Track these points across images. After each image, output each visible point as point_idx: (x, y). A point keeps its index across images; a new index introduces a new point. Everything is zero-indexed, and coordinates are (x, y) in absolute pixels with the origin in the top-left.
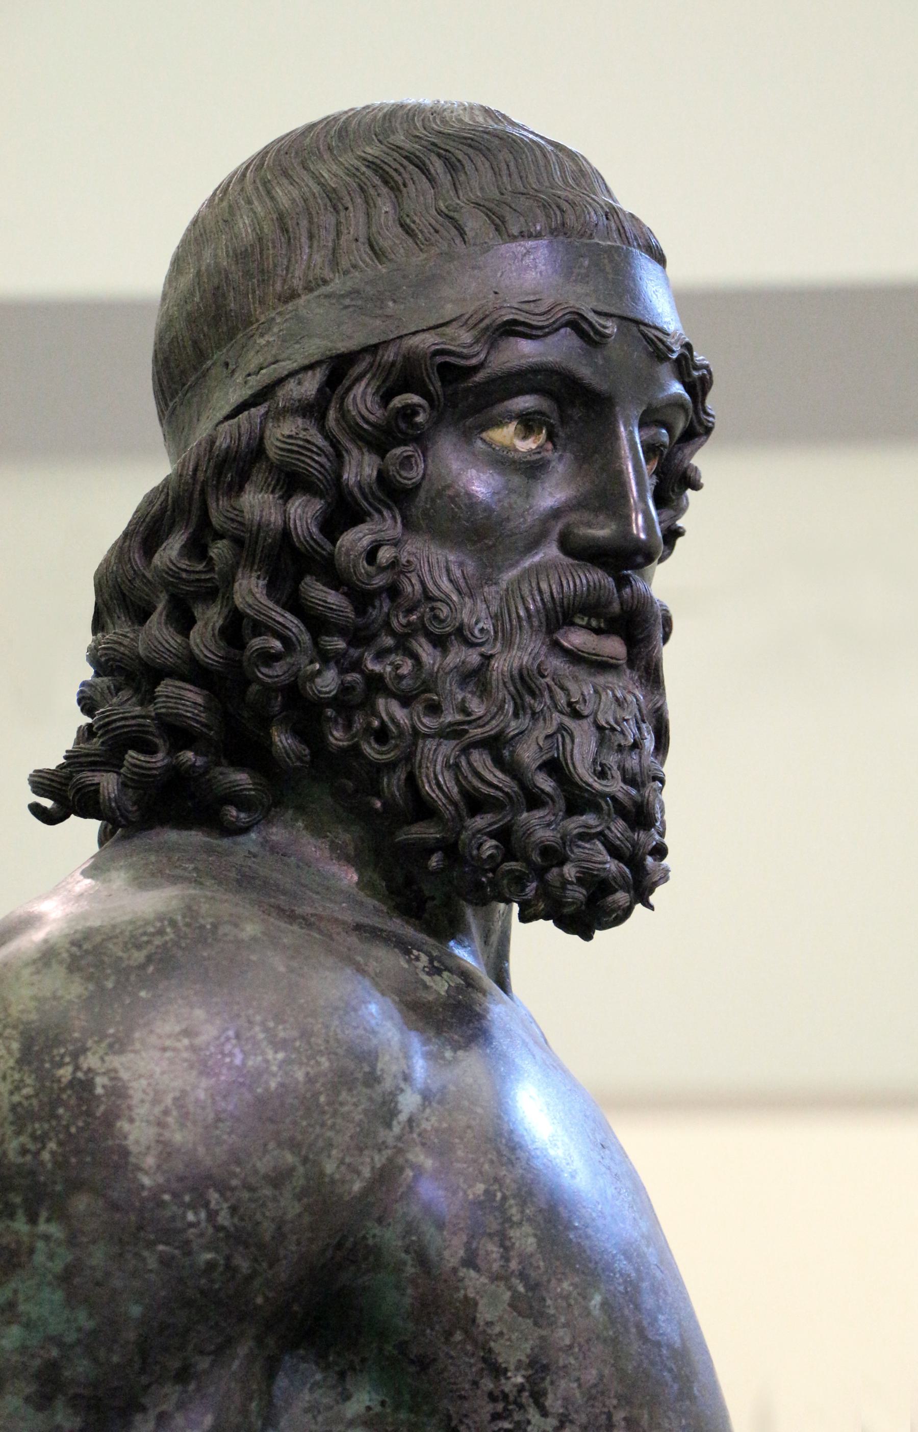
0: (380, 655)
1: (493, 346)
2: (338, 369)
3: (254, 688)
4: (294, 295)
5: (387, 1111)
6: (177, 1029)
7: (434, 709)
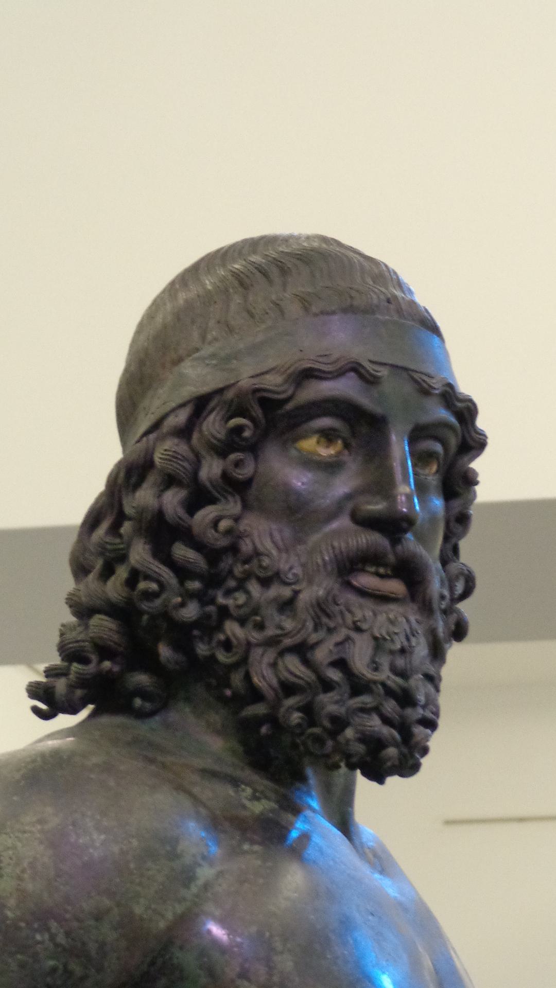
0: (228, 593)
2: (200, 405)
3: (145, 617)
4: (180, 360)
5: (187, 877)
6: (34, 819)
7: (260, 627)
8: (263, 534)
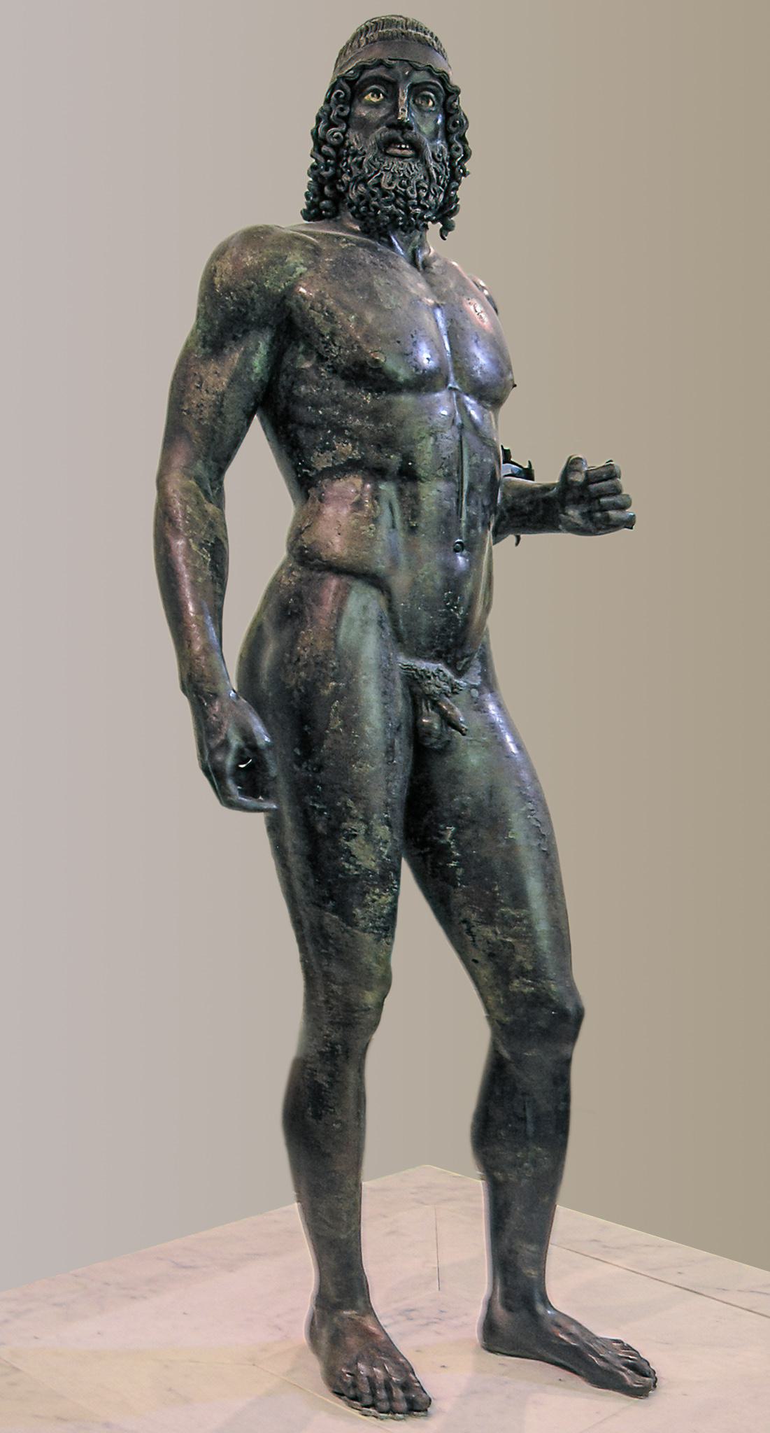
1: (361, 74)
8: (354, 137)
